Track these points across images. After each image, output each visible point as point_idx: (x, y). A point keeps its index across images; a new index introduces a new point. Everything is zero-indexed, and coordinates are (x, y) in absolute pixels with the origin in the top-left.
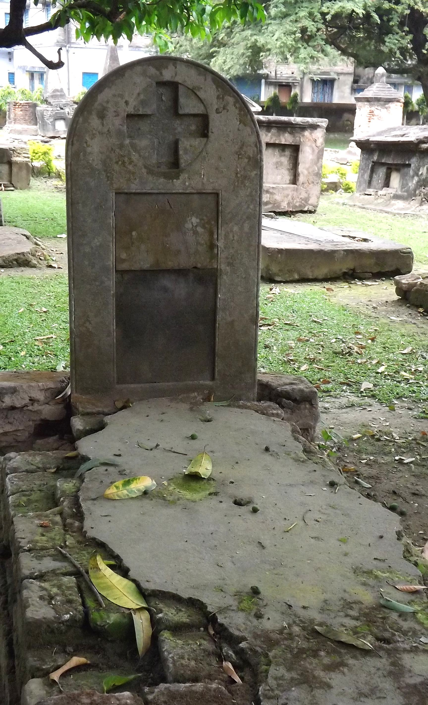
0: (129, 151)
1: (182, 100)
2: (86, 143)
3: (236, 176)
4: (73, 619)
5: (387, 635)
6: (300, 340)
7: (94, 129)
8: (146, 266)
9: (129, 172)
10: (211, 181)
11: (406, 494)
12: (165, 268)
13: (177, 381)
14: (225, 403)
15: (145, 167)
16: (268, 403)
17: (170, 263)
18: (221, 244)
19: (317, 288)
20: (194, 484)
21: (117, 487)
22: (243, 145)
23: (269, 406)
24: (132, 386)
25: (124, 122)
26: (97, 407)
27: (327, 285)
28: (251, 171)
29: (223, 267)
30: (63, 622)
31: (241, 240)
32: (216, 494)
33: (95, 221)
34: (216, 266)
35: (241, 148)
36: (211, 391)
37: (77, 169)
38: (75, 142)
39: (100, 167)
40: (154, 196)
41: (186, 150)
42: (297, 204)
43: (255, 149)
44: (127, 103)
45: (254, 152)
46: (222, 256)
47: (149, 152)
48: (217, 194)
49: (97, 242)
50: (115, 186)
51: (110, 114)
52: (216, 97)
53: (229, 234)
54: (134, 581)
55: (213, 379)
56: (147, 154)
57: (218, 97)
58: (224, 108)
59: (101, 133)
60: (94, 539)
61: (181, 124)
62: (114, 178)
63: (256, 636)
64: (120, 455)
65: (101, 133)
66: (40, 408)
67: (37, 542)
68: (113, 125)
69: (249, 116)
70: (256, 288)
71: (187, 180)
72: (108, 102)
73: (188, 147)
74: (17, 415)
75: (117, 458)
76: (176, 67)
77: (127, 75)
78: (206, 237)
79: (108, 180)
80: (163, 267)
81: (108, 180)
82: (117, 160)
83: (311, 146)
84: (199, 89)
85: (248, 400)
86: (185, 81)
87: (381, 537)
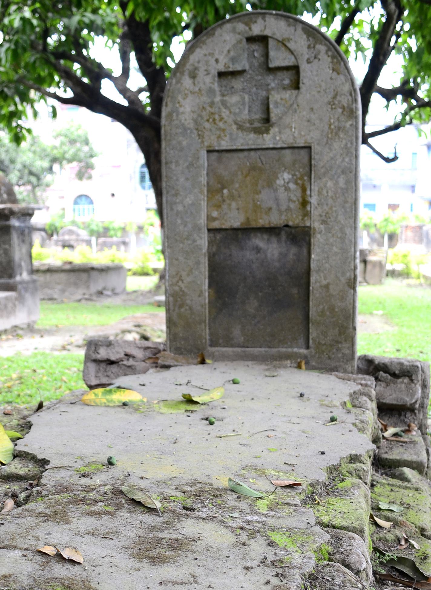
0: (219, 108)
1: (272, 53)
2: (179, 103)
3: (330, 128)
7: (186, 89)
8: (237, 224)
9: (220, 129)
10: (303, 133)
12: (255, 226)
13: (270, 347)
15: (236, 123)
17: (260, 221)
18: (314, 200)
22: (336, 95)
24: (224, 349)
25: (214, 80)
28: (346, 122)
29: (317, 225)
31: (336, 196)
33: (187, 179)
34: (308, 224)
35: (334, 97)
37: (171, 130)
38: (169, 103)
39: (192, 125)
40: (246, 153)
41: (276, 103)
43: (350, 98)
44: (217, 61)
45: (348, 100)
46: (315, 213)
47: (239, 108)
48: (310, 148)
49: (188, 201)
50: (206, 144)
51: (201, 73)
52: (306, 46)
53: (322, 189)
56: (237, 110)
57: (309, 47)
58: (315, 58)
59: (193, 93)
61: (274, 80)
62: (205, 136)
65: (193, 93)
68: (204, 84)
69: (342, 63)
70: (353, 249)
71: (278, 134)
72: (199, 62)
73: (279, 100)
76: (265, 21)
78: (299, 194)
79: (199, 139)
80: (254, 225)
81: (199, 139)
82: (208, 118)
84: (289, 40)
86: (274, 34)
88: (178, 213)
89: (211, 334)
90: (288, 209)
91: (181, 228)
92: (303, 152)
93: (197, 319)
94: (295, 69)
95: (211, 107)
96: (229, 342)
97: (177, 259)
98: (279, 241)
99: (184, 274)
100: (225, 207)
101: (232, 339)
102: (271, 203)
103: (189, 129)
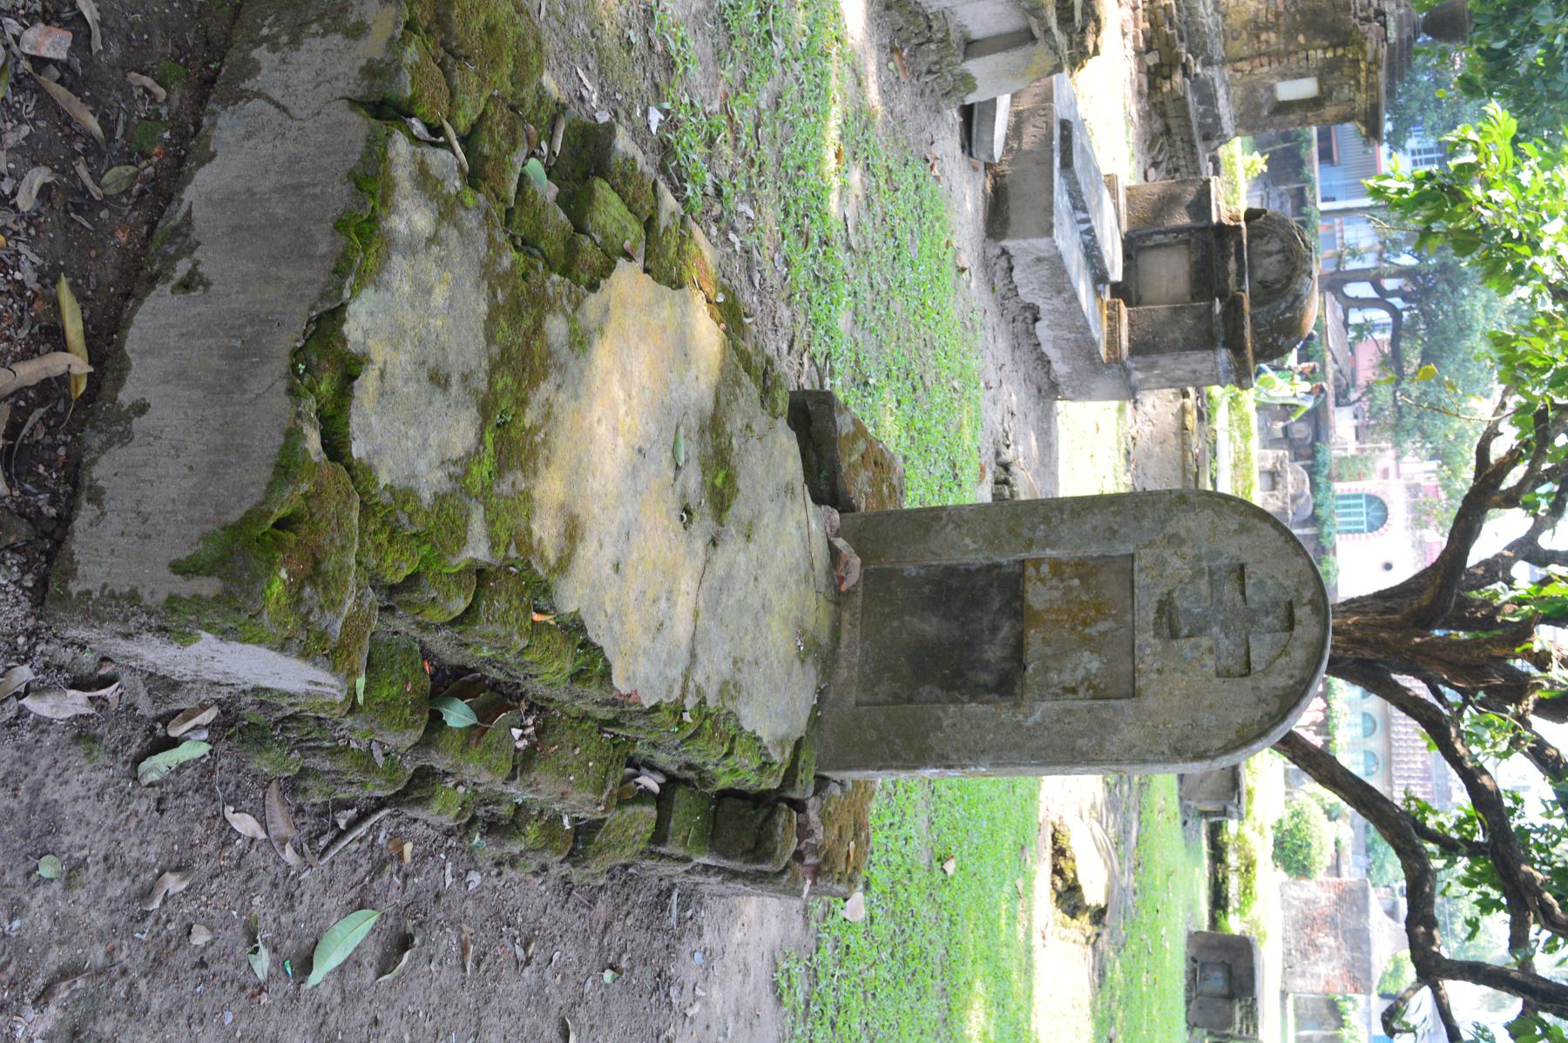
33: (1095, 529)
51: (1245, 540)
98: (1004, 659)
100: (1055, 582)
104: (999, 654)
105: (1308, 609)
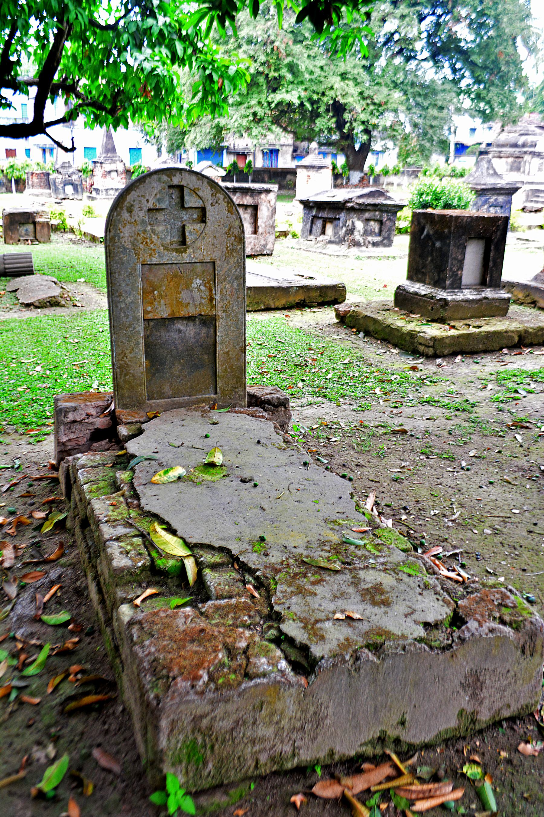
1: (186, 198)
4: (144, 565)
5: (348, 560)
6: (269, 356)
8: (165, 315)
9: (151, 249)
11: (352, 466)
14: (225, 410)
16: (255, 408)
18: (218, 297)
19: (278, 315)
20: (212, 470)
21: (160, 476)
23: (256, 410)
24: (158, 401)
26: (135, 417)
27: (286, 312)
29: (220, 313)
30: (137, 568)
32: (228, 476)
35: (230, 229)
36: (215, 401)
39: (130, 246)
40: (169, 266)
41: (190, 232)
42: (258, 249)
46: (219, 305)
48: (214, 263)
49: (129, 300)
50: (141, 260)
51: (136, 209)
54: (181, 538)
55: (216, 393)
59: (130, 223)
60: (149, 512)
63: (266, 567)
64: (157, 452)
65: (130, 223)
66: (94, 420)
67: (110, 516)
68: (139, 217)
72: (134, 201)
74: (78, 426)
75: (156, 454)
77: (147, 181)
78: (207, 293)
80: (177, 315)
83: (266, 206)
84: (199, 189)
85: (241, 406)
87: (340, 498)
88: (121, 309)
89: (148, 392)
90: (201, 303)
91: (124, 319)
92: (208, 265)
93: (139, 382)
94: (203, 210)
95: (144, 234)
96: (161, 396)
97: (122, 342)
99: (127, 352)
100: (156, 303)
101: (164, 393)
102: (189, 300)
103: (128, 249)
104: (191, 328)
105: (173, 178)
